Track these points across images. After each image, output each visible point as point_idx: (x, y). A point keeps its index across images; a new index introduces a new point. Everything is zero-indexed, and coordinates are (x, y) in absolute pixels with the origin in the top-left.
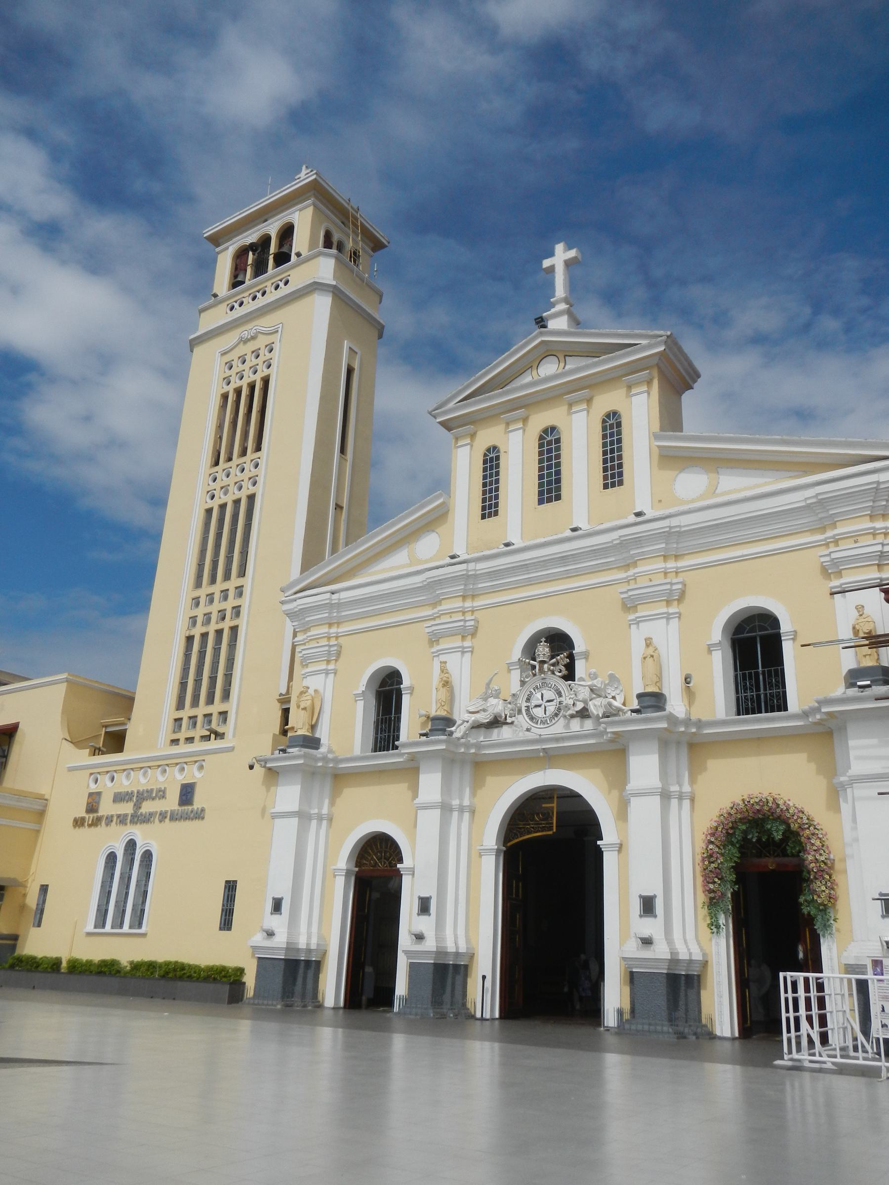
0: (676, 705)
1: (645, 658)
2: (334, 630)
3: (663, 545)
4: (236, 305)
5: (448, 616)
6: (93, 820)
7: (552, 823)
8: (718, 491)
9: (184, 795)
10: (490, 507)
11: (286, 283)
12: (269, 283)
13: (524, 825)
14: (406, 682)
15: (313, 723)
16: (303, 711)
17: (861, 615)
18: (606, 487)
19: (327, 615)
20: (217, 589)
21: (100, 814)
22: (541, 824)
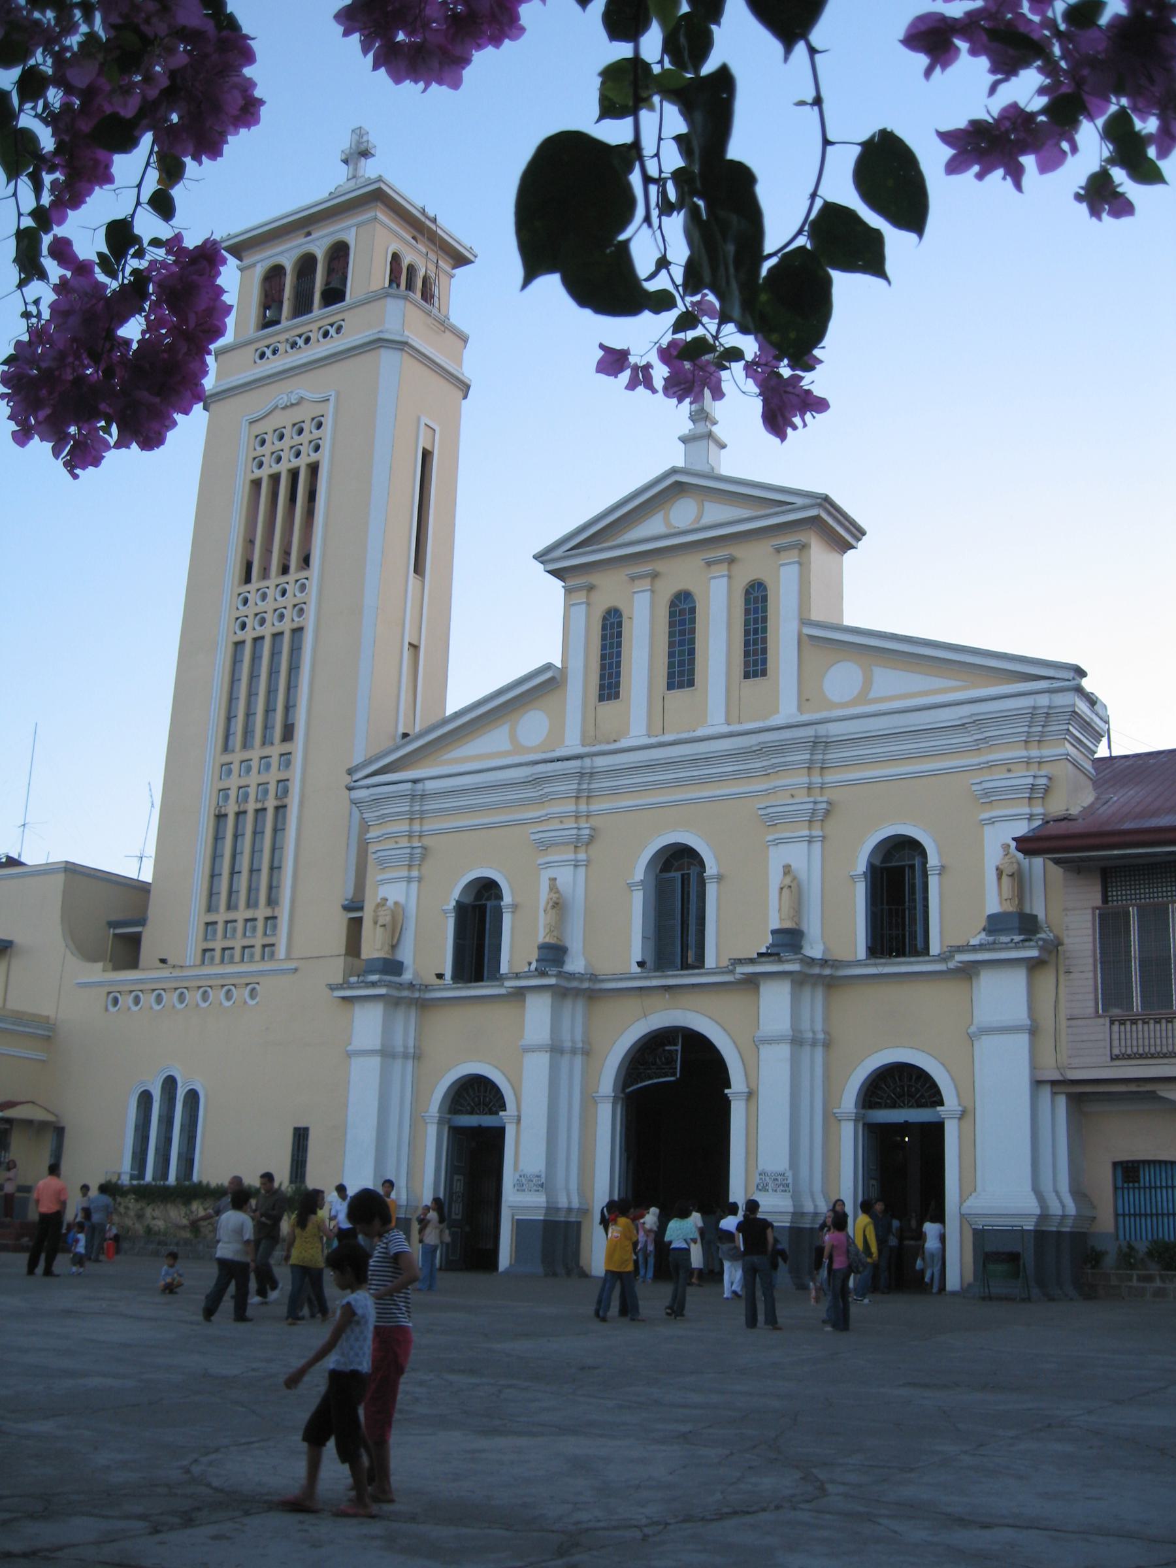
1: (782, 888)
3: (808, 756)
5: (557, 820)
7: (676, 1068)
8: (872, 695)
10: (610, 686)
11: (339, 330)
12: (314, 327)
13: (645, 1069)
15: (394, 943)
16: (382, 928)
17: (1006, 855)
18: (747, 676)
19: (407, 808)
20: (255, 754)
22: (664, 1069)
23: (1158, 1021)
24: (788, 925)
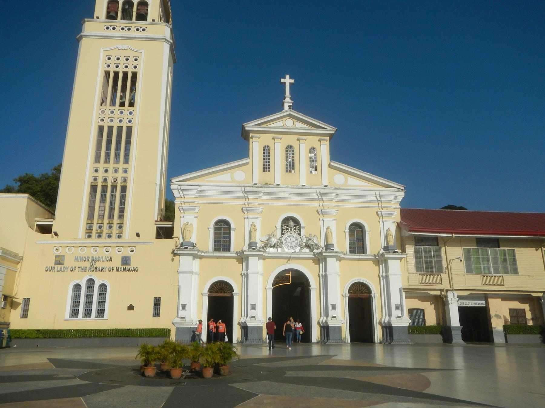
0: (336, 248)
2: (197, 201)
4: (111, 28)
6: (61, 268)
9: (125, 261)
12: (133, 26)
14: (233, 226)
19: (195, 194)
21: (66, 265)
23: (430, 275)
24: (330, 243)
